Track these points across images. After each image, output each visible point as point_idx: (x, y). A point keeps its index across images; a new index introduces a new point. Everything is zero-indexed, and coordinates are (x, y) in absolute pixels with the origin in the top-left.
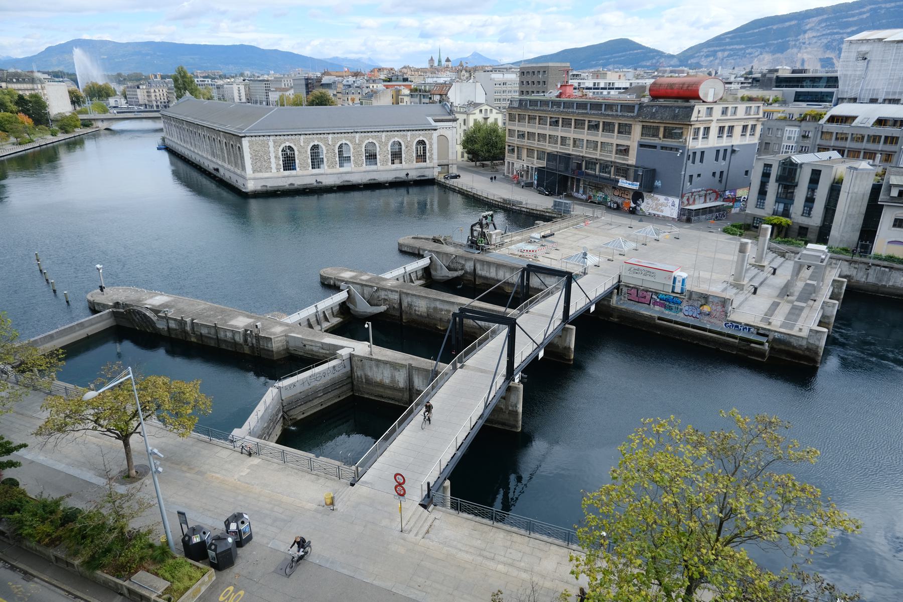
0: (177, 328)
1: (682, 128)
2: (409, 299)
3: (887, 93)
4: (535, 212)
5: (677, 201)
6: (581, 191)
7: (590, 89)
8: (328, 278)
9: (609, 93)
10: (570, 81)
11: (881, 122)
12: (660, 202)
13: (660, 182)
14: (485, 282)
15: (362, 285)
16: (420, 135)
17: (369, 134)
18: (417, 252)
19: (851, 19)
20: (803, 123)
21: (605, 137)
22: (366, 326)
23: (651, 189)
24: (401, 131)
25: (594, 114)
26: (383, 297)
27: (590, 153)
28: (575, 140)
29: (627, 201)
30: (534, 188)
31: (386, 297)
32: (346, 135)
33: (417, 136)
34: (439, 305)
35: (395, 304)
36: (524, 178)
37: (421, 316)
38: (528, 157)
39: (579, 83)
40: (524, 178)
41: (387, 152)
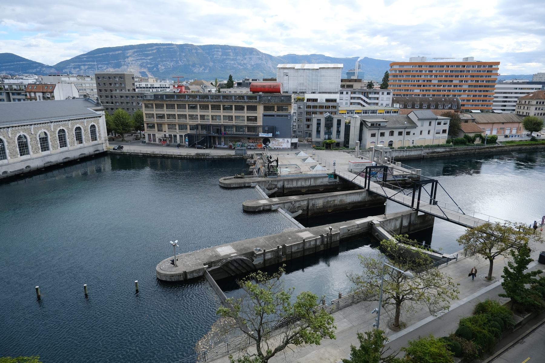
0: (272, 257)
1: (287, 106)
2: (313, 202)
3: (300, 89)
4: (224, 157)
5: (289, 140)
6: (223, 143)
7: (144, 88)
8: (259, 206)
9: (152, 90)
10: (136, 83)
11: (327, 100)
12: (280, 142)
14: (290, 190)
15: (284, 203)
16: (92, 121)
17: (60, 123)
18: (243, 185)
19: (148, 52)
20: (298, 102)
21: (238, 113)
23: (275, 136)
24: (80, 119)
25: (227, 102)
26: (297, 206)
27: (227, 122)
28: (212, 116)
29: (260, 144)
30: (186, 147)
31: (299, 205)
32: (44, 125)
33: (90, 122)
34: (329, 199)
35: (305, 207)
36: (168, 142)
37: (320, 209)
38: (169, 129)
39: (139, 84)
40: (168, 142)
41: (73, 135)
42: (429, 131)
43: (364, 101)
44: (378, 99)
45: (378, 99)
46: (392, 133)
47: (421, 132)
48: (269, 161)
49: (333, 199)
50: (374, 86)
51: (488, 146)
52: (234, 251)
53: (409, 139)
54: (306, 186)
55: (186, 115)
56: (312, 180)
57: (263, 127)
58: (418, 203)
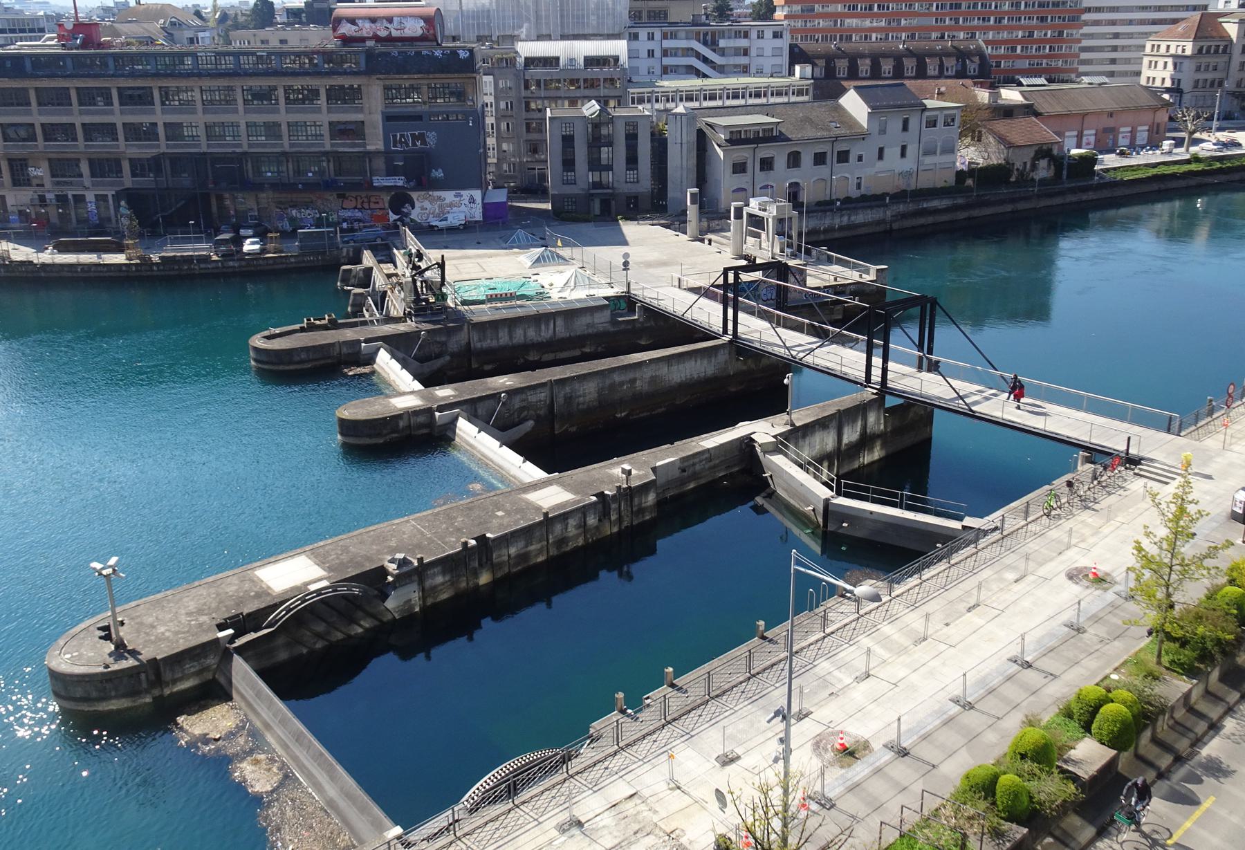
2: (568, 389)
5: (477, 194)
11: (591, 61)
12: (447, 201)
13: (440, 170)
22: (786, 381)
23: (425, 183)
26: (517, 406)
29: (379, 213)
31: (524, 404)
34: (617, 378)
42: (904, 149)
43: (705, 60)
44: (746, 52)
45: (746, 52)
46: (794, 160)
47: (881, 151)
48: (415, 267)
49: (630, 375)
50: (731, 10)
51: (1073, 185)
52: (319, 572)
53: (847, 175)
54: (540, 339)
55: (112, 127)
56: (560, 322)
57: (387, 154)
58: (885, 371)
